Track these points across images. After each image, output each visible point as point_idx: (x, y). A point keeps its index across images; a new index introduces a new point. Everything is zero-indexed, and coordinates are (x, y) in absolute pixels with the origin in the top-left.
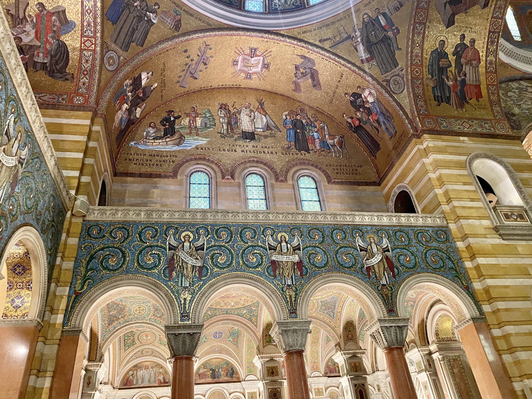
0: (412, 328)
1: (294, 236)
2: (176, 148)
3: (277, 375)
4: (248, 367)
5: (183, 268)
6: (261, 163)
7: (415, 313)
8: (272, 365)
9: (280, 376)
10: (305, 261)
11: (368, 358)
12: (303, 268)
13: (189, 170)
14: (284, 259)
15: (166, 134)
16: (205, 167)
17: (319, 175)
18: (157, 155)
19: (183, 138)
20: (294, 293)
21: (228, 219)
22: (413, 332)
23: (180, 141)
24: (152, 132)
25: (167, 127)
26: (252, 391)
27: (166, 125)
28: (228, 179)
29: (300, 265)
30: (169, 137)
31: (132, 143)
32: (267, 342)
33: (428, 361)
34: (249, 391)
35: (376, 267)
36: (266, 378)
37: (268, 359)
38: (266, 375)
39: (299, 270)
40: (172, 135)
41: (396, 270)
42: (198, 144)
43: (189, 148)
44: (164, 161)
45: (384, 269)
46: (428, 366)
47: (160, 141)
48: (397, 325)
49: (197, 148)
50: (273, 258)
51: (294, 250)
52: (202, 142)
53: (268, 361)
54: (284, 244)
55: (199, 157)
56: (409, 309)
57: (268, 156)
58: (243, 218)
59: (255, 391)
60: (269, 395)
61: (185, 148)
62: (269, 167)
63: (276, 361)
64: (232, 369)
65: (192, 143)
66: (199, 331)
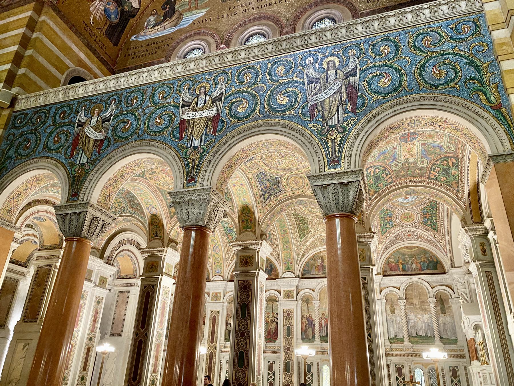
0: (460, 199)
1: (217, 84)
2: (174, 29)
3: (251, 265)
4: (285, 264)
5: (85, 144)
6: (264, 18)
7: (462, 175)
8: (246, 253)
9: (254, 266)
10: (224, 115)
11: (446, 253)
12: (220, 123)
13: (182, 51)
14: (198, 115)
15: (165, 18)
16: (199, 42)
17: (342, 12)
18: (154, 43)
19: (181, 17)
20: (199, 156)
21: (143, 80)
22: (462, 204)
23: (178, 20)
24: (152, 20)
25: (167, 9)
26: (289, 289)
27: (167, 8)
28: (222, 48)
29: (216, 118)
30: (167, 21)
31: (133, 38)
32: (244, 228)
33: (482, 245)
34: (286, 289)
35: (327, 102)
36: (239, 268)
37: (241, 248)
38: (238, 265)
39: (213, 127)
40: (170, 18)
41: (359, 101)
42: (195, 18)
43: (186, 26)
44: (159, 47)
45: (340, 103)
46: (480, 254)
47: (159, 27)
48: (339, 181)
49: (194, 23)
50: (185, 117)
51: (213, 102)
52: (200, 14)
53: (241, 250)
54: (202, 96)
55: (196, 31)
56: (453, 171)
57: (275, 8)
58: (159, 75)
59: (292, 289)
60: (239, 288)
61: (182, 27)
62: (273, 21)
63: (251, 249)
64: (271, 266)
65: (189, 19)
66: (85, 210)
